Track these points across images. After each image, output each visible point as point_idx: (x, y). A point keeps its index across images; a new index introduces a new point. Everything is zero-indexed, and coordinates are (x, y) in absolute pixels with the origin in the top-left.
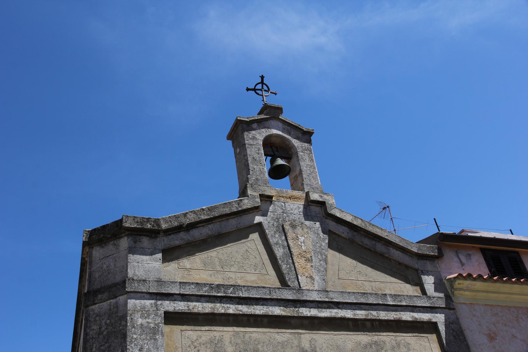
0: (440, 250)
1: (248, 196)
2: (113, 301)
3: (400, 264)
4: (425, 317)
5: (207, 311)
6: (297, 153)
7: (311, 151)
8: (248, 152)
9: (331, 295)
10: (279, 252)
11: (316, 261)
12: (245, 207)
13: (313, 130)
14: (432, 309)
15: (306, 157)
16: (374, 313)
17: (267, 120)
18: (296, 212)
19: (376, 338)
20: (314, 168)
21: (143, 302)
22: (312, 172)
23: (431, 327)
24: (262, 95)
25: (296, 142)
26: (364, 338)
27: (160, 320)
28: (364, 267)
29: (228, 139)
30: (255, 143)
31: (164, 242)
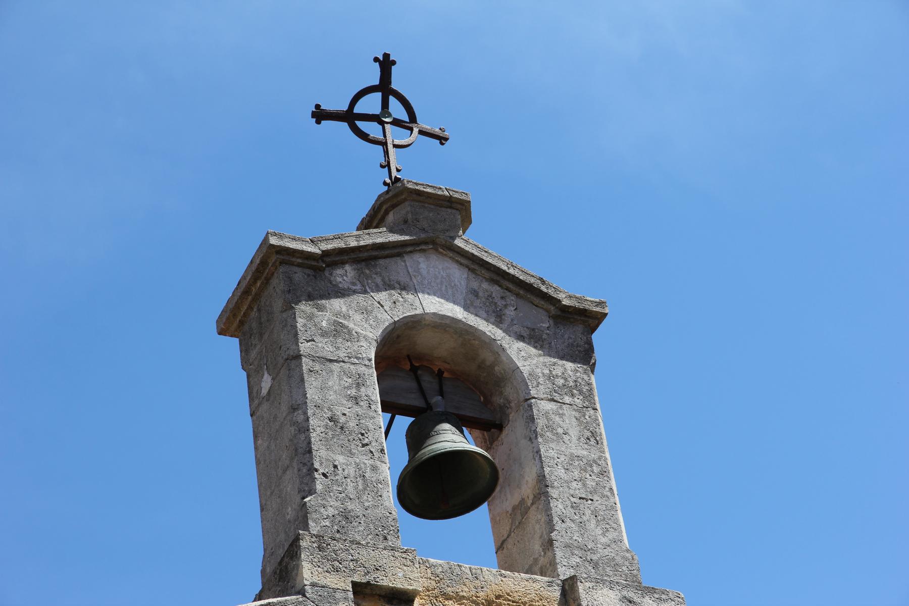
1: (302, 592)
7: (588, 396)
8: (312, 393)
13: (601, 304)
15: (568, 422)
17: (399, 255)
20: (603, 473)
22: (594, 491)
24: (384, 144)
25: (524, 357)
29: (220, 334)
30: (342, 354)
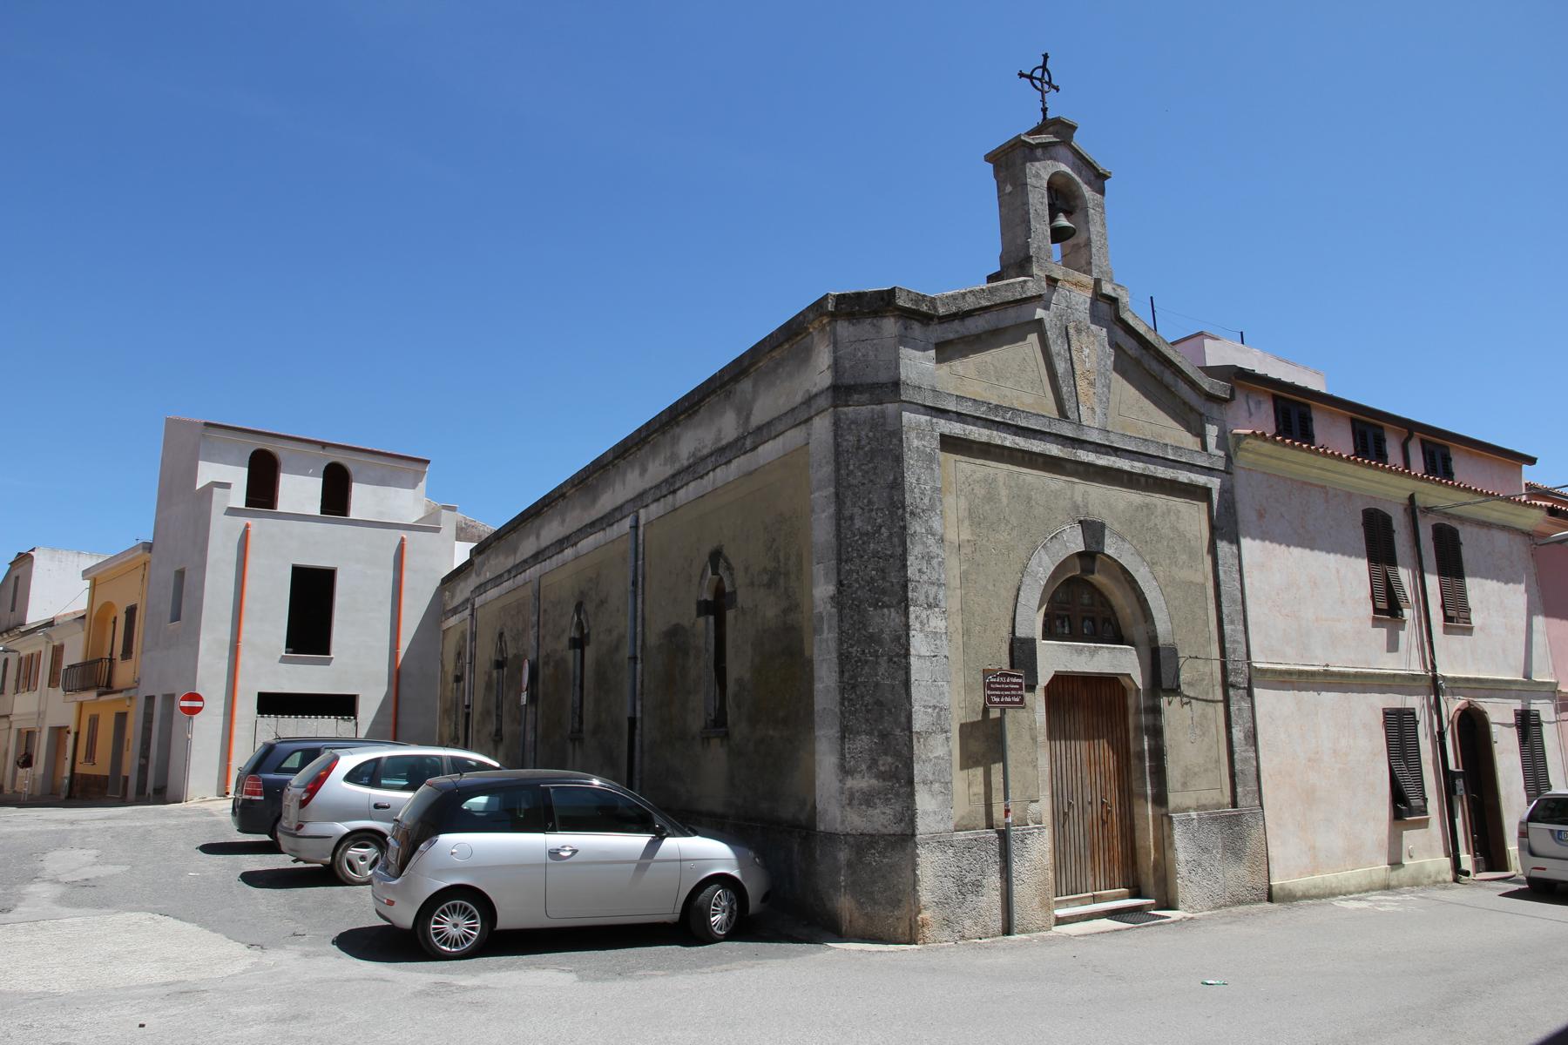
0: (1232, 391)
2: (877, 408)
3: (1185, 403)
4: (1201, 479)
5: (984, 439)
6: (1085, 209)
9: (1112, 437)
10: (1061, 367)
11: (1099, 389)
12: (1029, 294)
14: (1209, 471)
16: (1152, 467)
18: (1081, 308)
19: (1148, 500)
21: (919, 417)
23: (1202, 494)
25: (1087, 191)
26: (1135, 497)
27: (936, 444)
28: (1147, 402)
31: (939, 332)
